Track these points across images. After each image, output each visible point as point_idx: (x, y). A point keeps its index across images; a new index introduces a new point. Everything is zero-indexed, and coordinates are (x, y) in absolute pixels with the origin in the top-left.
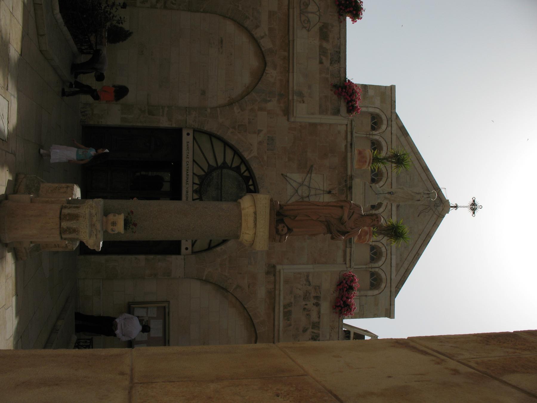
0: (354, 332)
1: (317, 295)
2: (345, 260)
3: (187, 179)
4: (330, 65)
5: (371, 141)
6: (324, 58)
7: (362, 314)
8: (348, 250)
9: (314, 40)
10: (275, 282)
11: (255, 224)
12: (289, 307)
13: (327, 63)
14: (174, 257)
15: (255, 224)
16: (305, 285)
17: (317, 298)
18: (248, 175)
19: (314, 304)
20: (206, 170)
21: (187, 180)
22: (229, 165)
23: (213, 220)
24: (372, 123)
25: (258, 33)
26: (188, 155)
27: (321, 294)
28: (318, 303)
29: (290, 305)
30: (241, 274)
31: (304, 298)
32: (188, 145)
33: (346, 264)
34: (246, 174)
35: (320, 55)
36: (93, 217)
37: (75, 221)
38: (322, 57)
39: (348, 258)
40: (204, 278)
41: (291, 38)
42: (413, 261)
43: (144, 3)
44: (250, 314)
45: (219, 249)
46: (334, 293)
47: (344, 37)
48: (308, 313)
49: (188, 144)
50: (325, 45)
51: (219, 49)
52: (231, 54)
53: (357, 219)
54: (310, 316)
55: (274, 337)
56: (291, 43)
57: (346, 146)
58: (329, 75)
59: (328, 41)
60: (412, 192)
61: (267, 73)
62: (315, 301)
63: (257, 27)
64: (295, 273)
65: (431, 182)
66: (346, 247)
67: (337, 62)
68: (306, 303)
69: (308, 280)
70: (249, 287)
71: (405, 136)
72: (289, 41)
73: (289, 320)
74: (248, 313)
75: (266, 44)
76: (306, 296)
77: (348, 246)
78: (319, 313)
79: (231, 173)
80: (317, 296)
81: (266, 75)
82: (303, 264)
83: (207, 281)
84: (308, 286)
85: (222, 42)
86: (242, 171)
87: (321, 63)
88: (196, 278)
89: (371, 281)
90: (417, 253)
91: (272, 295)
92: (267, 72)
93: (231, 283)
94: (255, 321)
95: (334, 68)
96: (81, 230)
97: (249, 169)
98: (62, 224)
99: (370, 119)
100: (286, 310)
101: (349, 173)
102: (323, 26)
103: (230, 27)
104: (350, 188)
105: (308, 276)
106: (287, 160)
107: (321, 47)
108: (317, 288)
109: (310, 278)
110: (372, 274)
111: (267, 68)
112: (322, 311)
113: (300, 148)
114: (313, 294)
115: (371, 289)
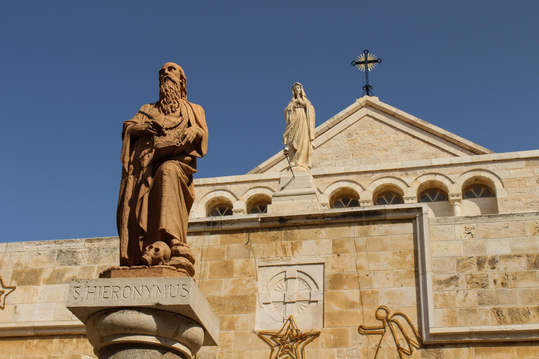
1: (475, 262)
4: (79, 265)
6: (68, 276)
9: (37, 293)
17: (480, 264)
19: (494, 268)
27: (472, 257)
28: (490, 261)
29: (498, 313)
31: (483, 287)
35: (60, 283)
42: (456, 143)
46: (469, 233)
47: (37, 245)
48: (510, 278)
50: (46, 275)
54: (516, 274)
57: (212, 233)
58: (94, 265)
59: (41, 271)
62: (487, 265)
64: (436, 306)
65: (329, 129)
67: (74, 254)
68: (493, 283)
76: (477, 283)
77: (383, 217)
78: (508, 257)
80: (477, 264)
84: (459, 281)
90: (443, 139)
100: (508, 319)
102: (16, 279)
105: (440, 282)
106: (233, 331)
107: (49, 281)
108: (461, 264)
109: (444, 277)
112: (507, 251)
114: (474, 270)
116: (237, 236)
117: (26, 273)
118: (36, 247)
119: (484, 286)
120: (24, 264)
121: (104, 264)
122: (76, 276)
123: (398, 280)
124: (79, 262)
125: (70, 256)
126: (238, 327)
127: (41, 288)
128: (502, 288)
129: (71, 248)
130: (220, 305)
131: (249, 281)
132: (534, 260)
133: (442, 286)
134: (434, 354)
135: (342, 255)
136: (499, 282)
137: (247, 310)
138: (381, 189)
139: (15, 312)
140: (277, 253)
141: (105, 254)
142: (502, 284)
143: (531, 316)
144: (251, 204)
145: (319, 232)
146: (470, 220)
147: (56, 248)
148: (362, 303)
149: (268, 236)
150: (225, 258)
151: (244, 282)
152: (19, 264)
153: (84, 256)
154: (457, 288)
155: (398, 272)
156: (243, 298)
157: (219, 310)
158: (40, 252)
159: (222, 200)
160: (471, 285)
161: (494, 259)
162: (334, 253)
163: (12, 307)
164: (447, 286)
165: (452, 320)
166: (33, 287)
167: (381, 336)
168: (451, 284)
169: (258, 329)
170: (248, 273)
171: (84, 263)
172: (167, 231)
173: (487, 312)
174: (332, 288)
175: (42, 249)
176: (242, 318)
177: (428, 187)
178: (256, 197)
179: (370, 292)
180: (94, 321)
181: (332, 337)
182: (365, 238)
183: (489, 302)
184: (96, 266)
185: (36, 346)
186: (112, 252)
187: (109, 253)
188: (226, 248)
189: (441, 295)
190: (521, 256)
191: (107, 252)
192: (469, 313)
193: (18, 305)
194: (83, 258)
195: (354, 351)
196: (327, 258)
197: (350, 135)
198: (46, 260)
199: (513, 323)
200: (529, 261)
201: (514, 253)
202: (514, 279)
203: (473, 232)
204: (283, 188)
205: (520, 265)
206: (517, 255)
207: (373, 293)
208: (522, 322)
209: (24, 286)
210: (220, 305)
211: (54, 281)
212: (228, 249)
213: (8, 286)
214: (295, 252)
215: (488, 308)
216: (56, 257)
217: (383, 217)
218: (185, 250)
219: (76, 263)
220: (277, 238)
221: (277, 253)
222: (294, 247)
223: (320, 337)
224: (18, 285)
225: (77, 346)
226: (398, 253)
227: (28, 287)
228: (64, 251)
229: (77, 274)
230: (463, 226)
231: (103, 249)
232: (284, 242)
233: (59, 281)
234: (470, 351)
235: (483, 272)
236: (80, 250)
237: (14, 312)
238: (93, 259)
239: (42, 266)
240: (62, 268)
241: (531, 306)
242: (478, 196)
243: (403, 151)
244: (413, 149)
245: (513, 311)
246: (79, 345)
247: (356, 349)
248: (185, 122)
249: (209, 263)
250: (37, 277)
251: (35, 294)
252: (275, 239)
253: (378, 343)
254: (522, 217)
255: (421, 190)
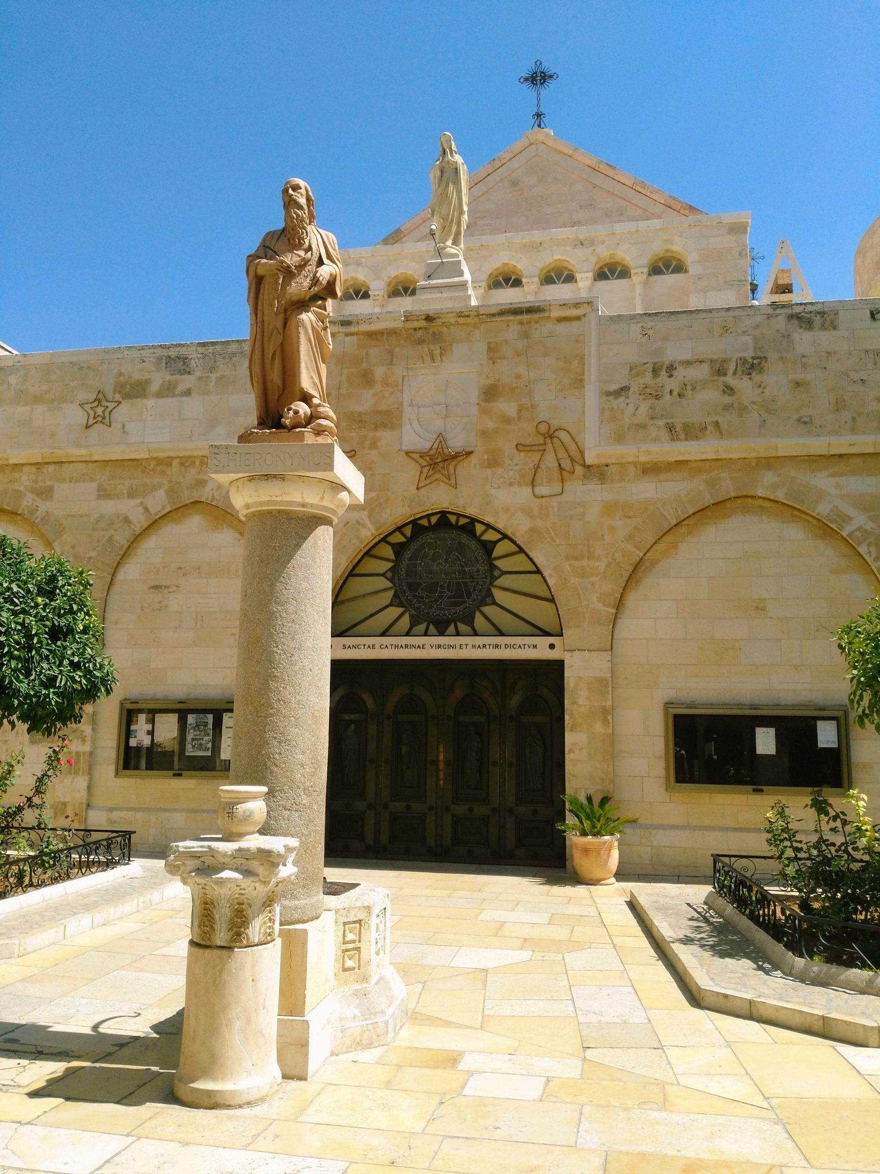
0: (772, 292)
2: (578, 318)
3: (415, 648)
4: (193, 374)
5: (389, 297)
6: (180, 388)
7: (740, 283)
8: (556, 313)
10: (623, 465)
11: (275, 476)
12: (675, 429)
13: (188, 381)
14: (567, 673)
15: (275, 476)
16: (627, 397)
17: (655, 371)
18: (410, 527)
19: (671, 376)
20: (401, 610)
21: (417, 647)
22: (390, 565)
23: (270, 576)
24: (357, 298)
25: (139, 520)
26: (369, 646)
29: (671, 428)
30: (603, 536)
31: (657, 399)
32: (349, 647)
33: (584, 315)
34: (408, 531)
35: (174, 396)
36: (206, 865)
37: (215, 911)
38: (176, 393)
39: (574, 312)
40: (613, 611)
41: (147, 456)
43: (85, 736)
44: (691, 513)
45: (551, 581)
46: (646, 334)
47: (139, 350)
48: (689, 388)
49: (347, 647)
50: (155, 387)
51: (169, 592)
52: (180, 568)
53: (289, 240)
55: (744, 458)
56: (155, 455)
57: (347, 335)
58: (210, 375)
59: (148, 382)
60: (439, 186)
61: (213, 497)
62: (663, 373)
63: (127, 521)
65: (489, 175)
66: (549, 317)
68: (669, 394)
69: (617, 393)
70: (629, 517)
71: (402, 235)
72: (153, 458)
73: (706, 428)
74: (689, 516)
75: (158, 502)
78: (688, 363)
79: (405, 563)
80: (653, 371)
81: (217, 500)
82: (583, 406)
83: (619, 605)
85: (156, 587)
86: (403, 539)
87: (188, 393)
88: (612, 626)
89: (669, 272)
91: (650, 470)
92: (210, 499)
93: (623, 556)
94: (708, 500)
95: (197, 366)
96: (237, 896)
97: (399, 529)
98: (219, 943)
99: (350, 303)
100: (682, 436)
101: (398, 324)
103: (130, 572)
104: (429, 318)
105: (608, 394)
106: (376, 452)
107: (159, 394)
108: (634, 371)
110: (655, 270)
111: (203, 500)
112: (687, 356)
113: (354, 427)
114: (648, 379)
115: (686, 271)
116: (377, 339)
117: (131, 385)
118: (138, 352)
119: (657, 397)
120: (126, 374)
121: (225, 374)
122: (191, 388)
123: (562, 391)
124: (193, 370)
125: (181, 363)
126: (381, 446)
127: (150, 402)
128: (678, 400)
129: (181, 353)
130: (361, 421)
131: (392, 394)
132: (718, 366)
133: (611, 398)
134: (598, 475)
135: (498, 361)
136: (675, 393)
137: (392, 427)
138: (550, 264)
139: (124, 431)
140: (423, 360)
141: (223, 361)
142: (679, 395)
143: (708, 432)
144: (393, 284)
145: (472, 333)
146: (648, 318)
147: (163, 354)
148: (519, 418)
149: (413, 339)
150: (365, 366)
151: (387, 394)
152: (121, 374)
153: (198, 364)
154: (628, 401)
155: (561, 382)
156: (388, 413)
157: (360, 427)
158: (145, 359)
159: (356, 279)
160: (641, 397)
161: (672, 366)
162: (490, 359)
163: (120, 426)
164: (616, 398)
165: (619, 438)
166: (139, 402)
167: (539, 455)
168: (621, 396)
169: (405, 448)
170: (391, 384)
171: (198, 374)
172: (306, 390)
173: (659, 428)
174: (486, 400)
175: (146, 355)
176: (386, 437)
177: (607, 261)
178: (397, 275)
179: (529, 405)
180: (238, 487)
181: (486, 457)
182: (525, 340)
183: (662, 415)
184: (213, 376)
185: (154, 470)
186: (231, 359)
187: (228, 360)
188: (365, 352)
189: (609, 408)
190: (704, 362)
191: (224, 358)
192: (638, 429)
193: (125, 423)
194: (197, 366)
195: (510, 473)
196: (481, 365)
197: (515, 183)
198: (153, 369)
199: (686, 439)
200: (712, 367)
201: (696, 358)
202: (693, 389)
203: (650, 332)
204: (429, 276)
205: (701, 372)
206: (700, 360)
207: (532, 406)
208: (697, 438)
209: (130, 400)
210: (361, 421)
211: (166, 395)
212: (367, 354)
213: (111, 400)
214: (444, 358)
215: (661, 423)
216: (164, 365)
217: (546, 314)
218: (325, 411)
219: (189, 372)
220: (423, 341)
221: (423, 360)
222: (443, 352)
223: (473, 458)
224: (123, 399)
225: (201, 470)
226: (563, 359)
227: (134, 401)
228: (173, 357)
229: (191, 386)
230: (640, 325)
231: (220, 354)
232: (432, 347)
233: (170, 394)
234: (637, 471)
235: (659, 380)
236: (192, 356)
237: (122, 431)
238: (209, 367)
239: (149, 377)
240: (173, 378)
241: (709, 420)
242: (668, 272)
243: (581, 207)
244: (593, 203)
245: (688, 426)
246: (203, 468)
247: (512, 470)
248: (315, 258)
249: (345, 371)
250: (144, 390)
251: (144, 410)
252: (420, 342)
253: (537, 463)
254: (710, 314)
255: (599, 265)
